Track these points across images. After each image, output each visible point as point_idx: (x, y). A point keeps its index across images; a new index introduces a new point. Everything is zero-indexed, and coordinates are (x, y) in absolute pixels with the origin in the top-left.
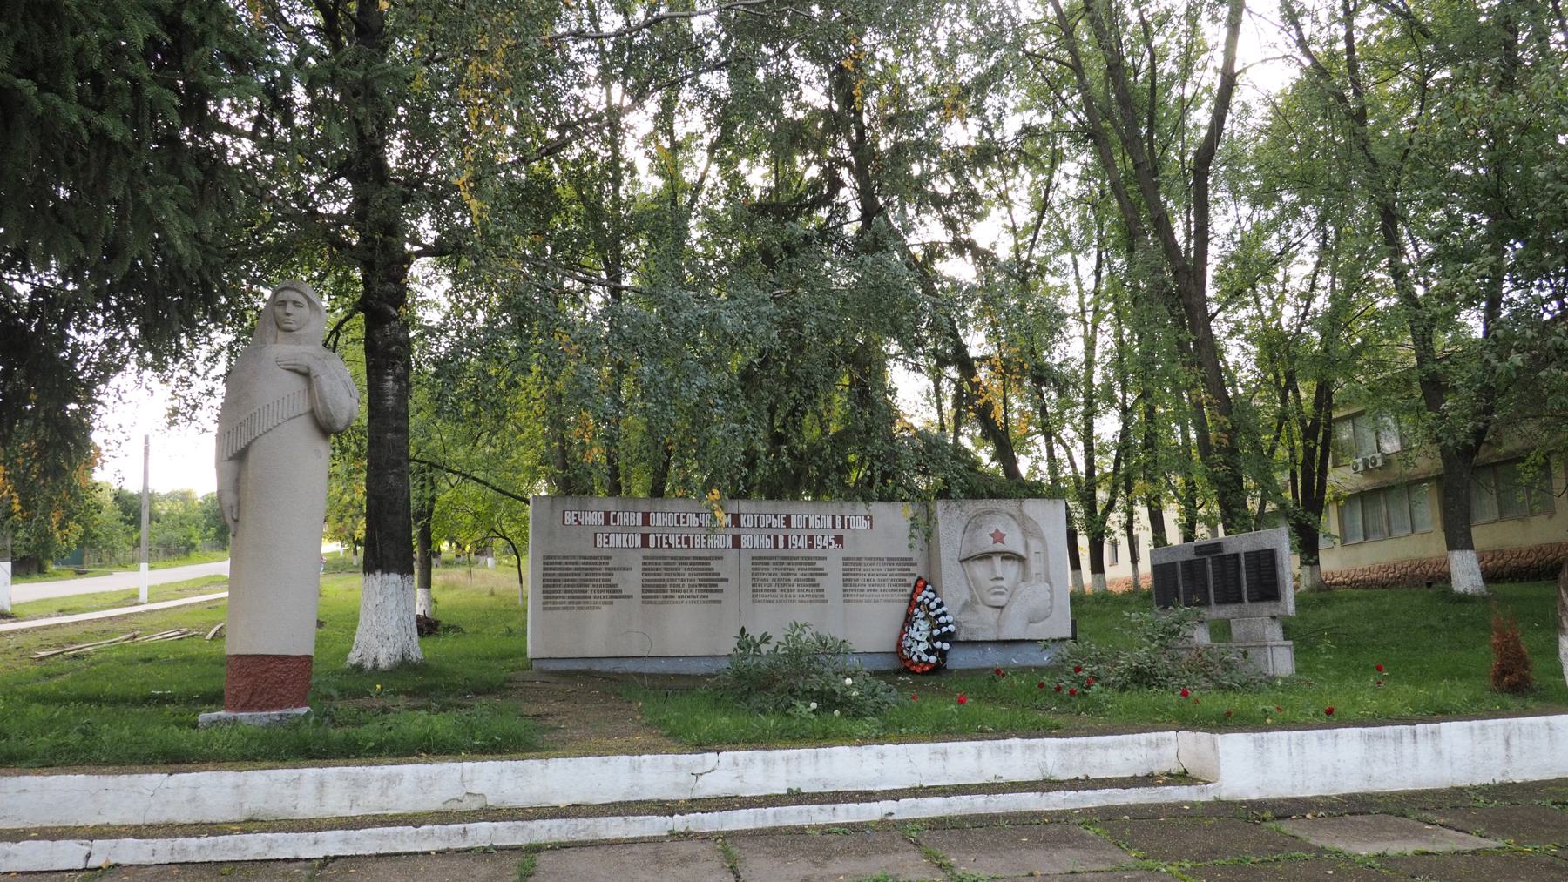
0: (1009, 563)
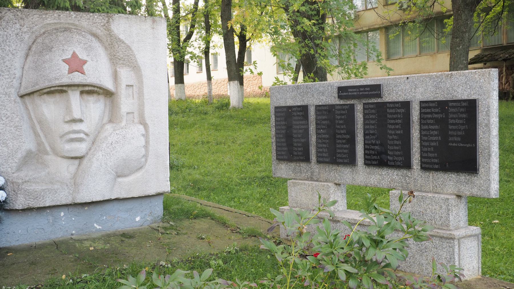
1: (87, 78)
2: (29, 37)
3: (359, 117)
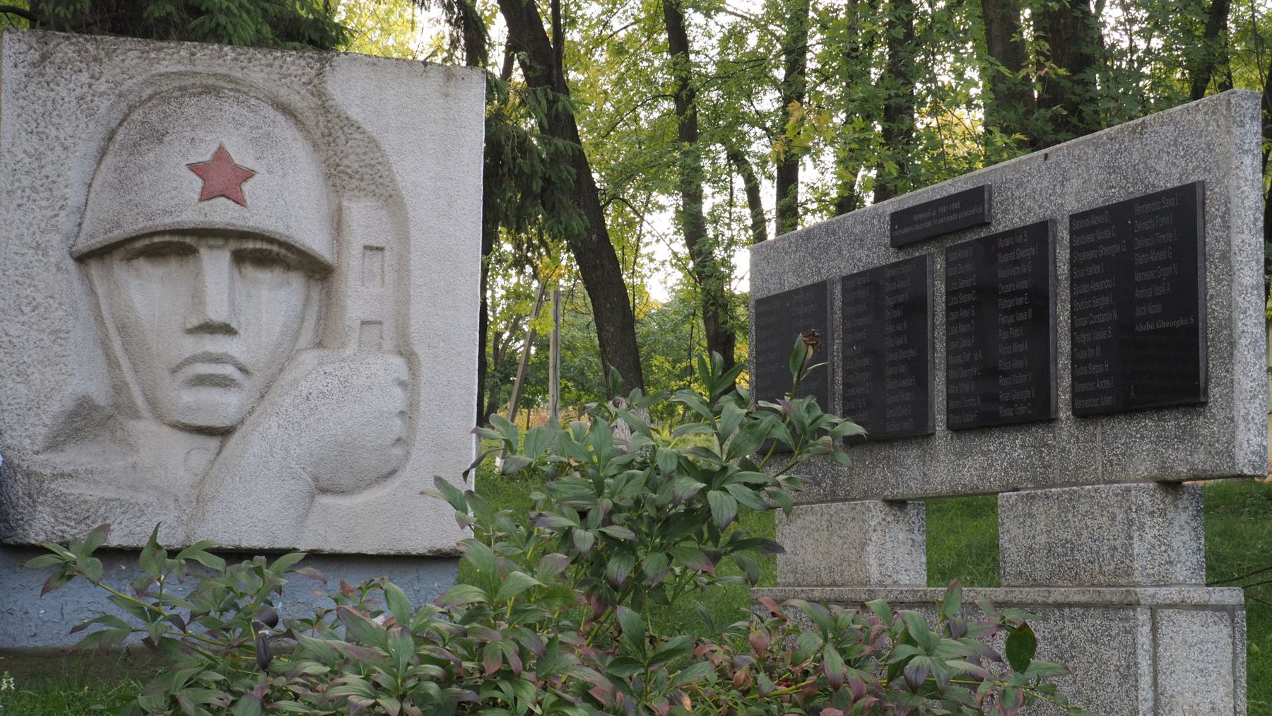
1: (248, 215)
2: (112, 107)
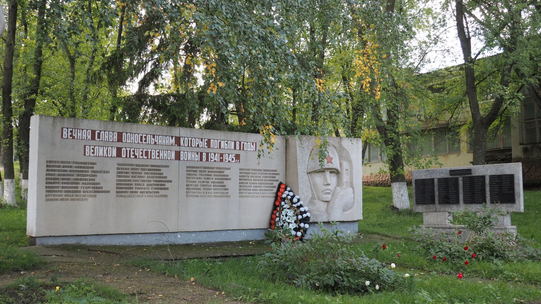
0: (332, 175)
3: (461, 183)
